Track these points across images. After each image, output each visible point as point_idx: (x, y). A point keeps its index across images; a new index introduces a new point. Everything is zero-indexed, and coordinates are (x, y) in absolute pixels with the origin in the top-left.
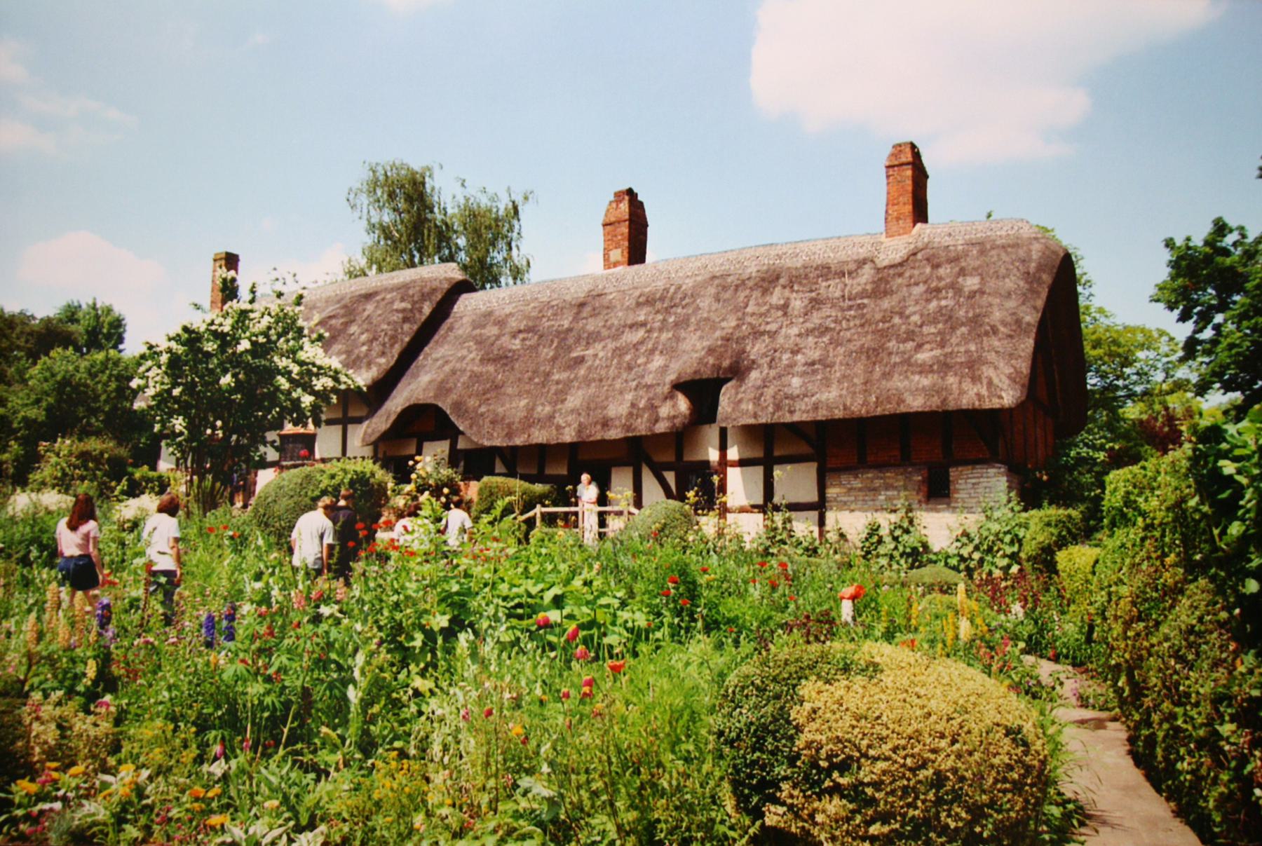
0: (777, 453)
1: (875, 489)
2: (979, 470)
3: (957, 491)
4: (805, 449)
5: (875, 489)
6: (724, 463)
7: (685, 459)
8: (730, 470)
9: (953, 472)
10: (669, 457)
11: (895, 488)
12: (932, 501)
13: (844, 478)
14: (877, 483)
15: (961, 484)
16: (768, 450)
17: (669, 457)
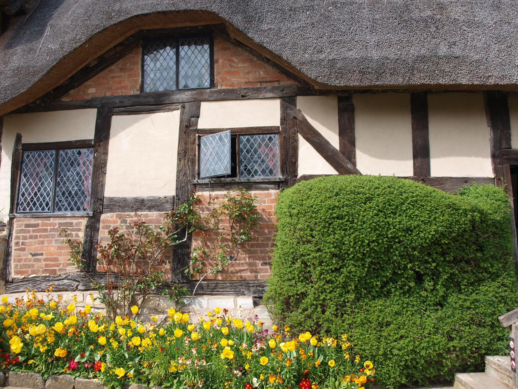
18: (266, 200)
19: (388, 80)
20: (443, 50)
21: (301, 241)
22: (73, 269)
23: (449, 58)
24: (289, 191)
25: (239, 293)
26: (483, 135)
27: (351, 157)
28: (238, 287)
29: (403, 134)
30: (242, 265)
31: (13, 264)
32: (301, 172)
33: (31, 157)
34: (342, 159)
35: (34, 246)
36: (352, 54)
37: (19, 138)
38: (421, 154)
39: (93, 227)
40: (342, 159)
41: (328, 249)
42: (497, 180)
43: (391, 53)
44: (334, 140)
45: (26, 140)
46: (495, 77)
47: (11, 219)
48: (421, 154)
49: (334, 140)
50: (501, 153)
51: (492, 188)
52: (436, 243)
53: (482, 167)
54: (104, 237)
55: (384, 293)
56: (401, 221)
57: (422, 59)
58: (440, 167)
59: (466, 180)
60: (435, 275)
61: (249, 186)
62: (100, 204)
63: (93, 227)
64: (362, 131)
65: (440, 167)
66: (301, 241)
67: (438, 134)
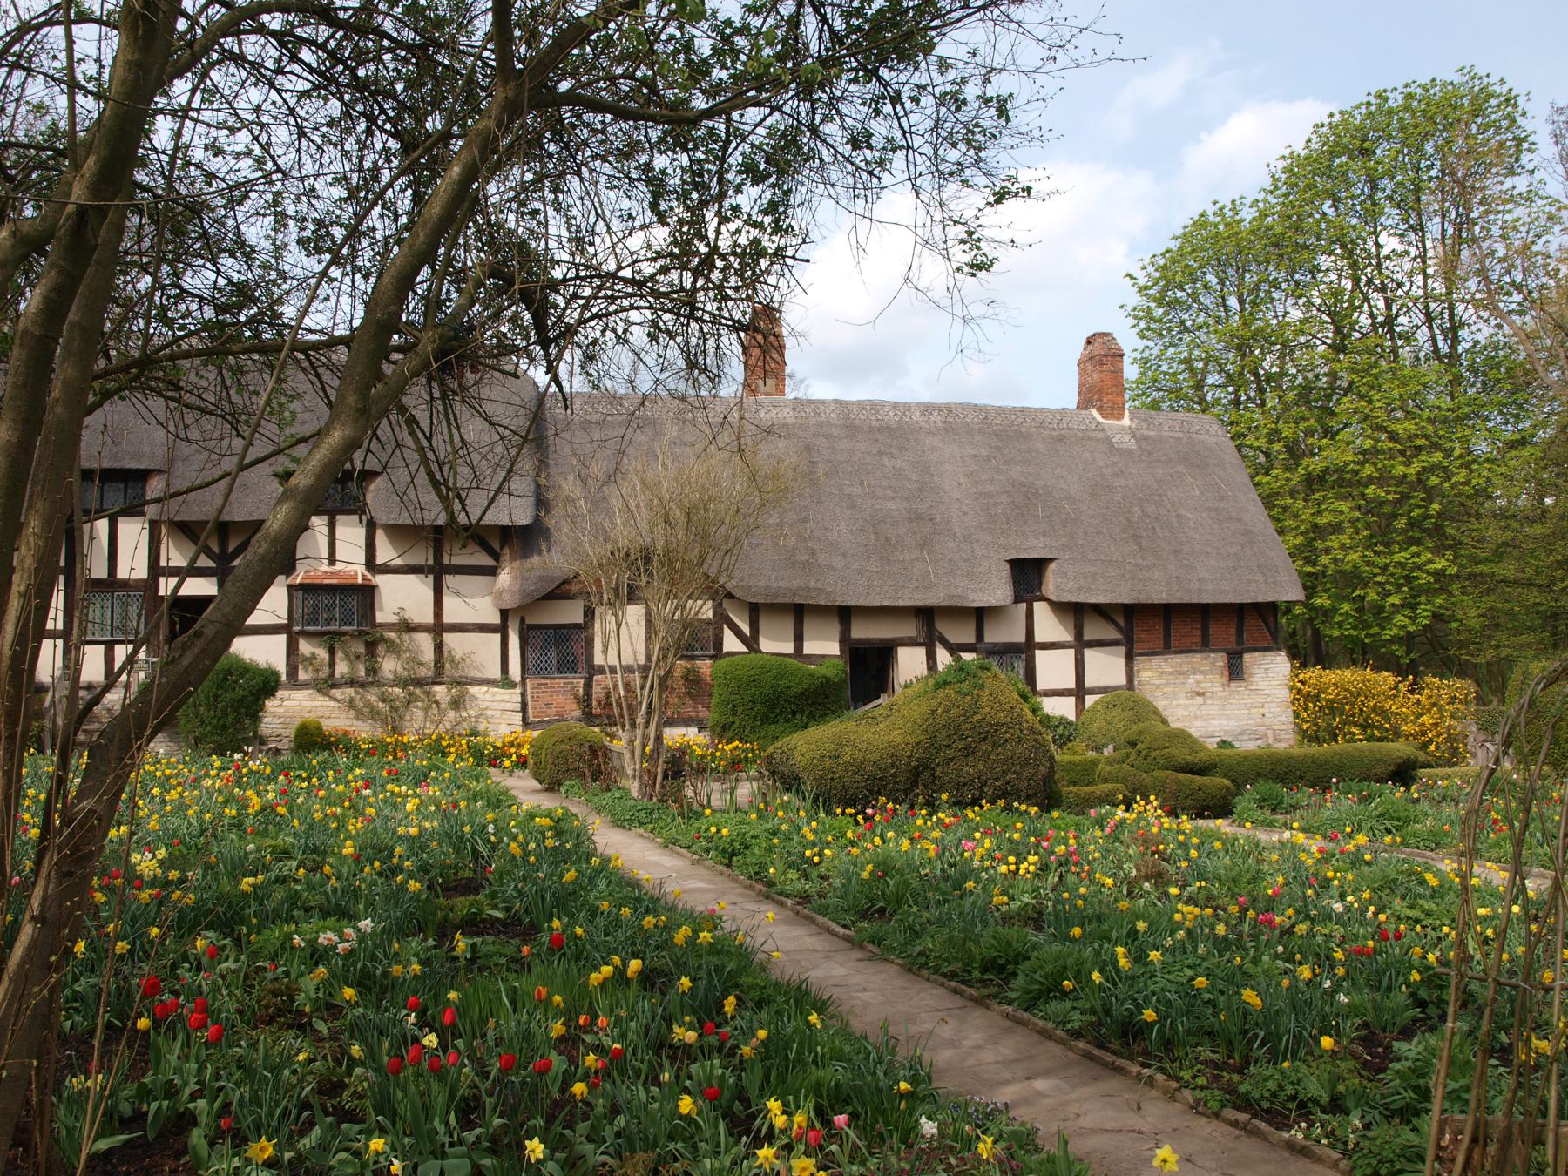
0: (1087, 637)
1: (1184, 673)
2: (1270, 656)
3: (1252, 675)
4: (1114, 634)
5: (1184, 673)
6: (1028, 648)
7: (987, 639)
8: (1037, 652)
9: (1247, 656)
10: (970, 638)
11: (1202, 673)
12: (1233, 684)
13: (1156, 661)
14: (1186, 667)
15: (1255, 669)
16: (1079, 634)
17: (970, 638)
18: (705, 667)
19: (781, 600)
20: (812, 584)
21: (732, 693)
22: (577, 713)
23: (815, 589)
24: (719, 663)
25: (687, 725)
26: (835, 629)
27: (757, 641)
28: (687, 722)
29: (788, 627)
30: (689, 709)
31: (530, 712)
32: (725, 649)
33: (531, 634)
34: (751, 642)
35: (546, 698)
36: (762, 584)
37: (523, 620)
38: (799, 639)
39: (588, 685)
40: (751, 642)
41: (747, 698)
42: (840, 657)
43: (783, 584)
44: (746, 630)
45: (528, 621)
46: (840, 601)
47: (524, 680)
48: (799, 639)
49: (746, 630)
50: (845, 640)
51: (837, 661)
52: (802, 694)
53: (833, 648)
54: (597, 691)
55: (775, 722)
56: (785, 683)
57: (800, 589)
58: (810, 648)
59: (824, 656)
60: (802, 712)
61: (693, 658)
62: (593, 670)
63: (588, 685)
64: (764, 625)
65: (810, 648)
66: (732, 693)
67: (809, 627)
